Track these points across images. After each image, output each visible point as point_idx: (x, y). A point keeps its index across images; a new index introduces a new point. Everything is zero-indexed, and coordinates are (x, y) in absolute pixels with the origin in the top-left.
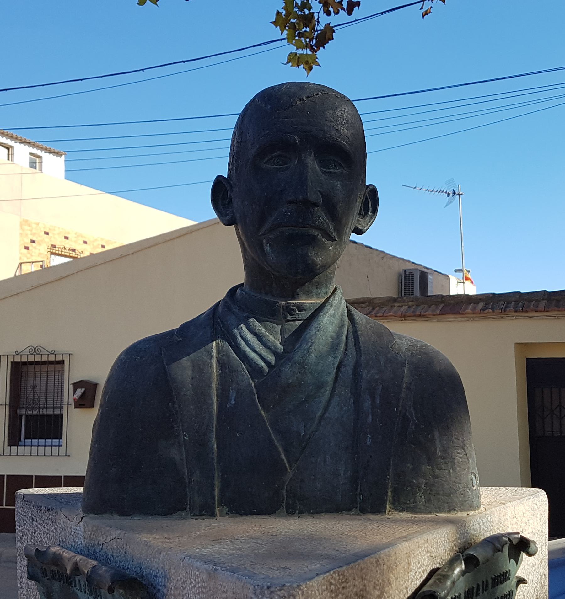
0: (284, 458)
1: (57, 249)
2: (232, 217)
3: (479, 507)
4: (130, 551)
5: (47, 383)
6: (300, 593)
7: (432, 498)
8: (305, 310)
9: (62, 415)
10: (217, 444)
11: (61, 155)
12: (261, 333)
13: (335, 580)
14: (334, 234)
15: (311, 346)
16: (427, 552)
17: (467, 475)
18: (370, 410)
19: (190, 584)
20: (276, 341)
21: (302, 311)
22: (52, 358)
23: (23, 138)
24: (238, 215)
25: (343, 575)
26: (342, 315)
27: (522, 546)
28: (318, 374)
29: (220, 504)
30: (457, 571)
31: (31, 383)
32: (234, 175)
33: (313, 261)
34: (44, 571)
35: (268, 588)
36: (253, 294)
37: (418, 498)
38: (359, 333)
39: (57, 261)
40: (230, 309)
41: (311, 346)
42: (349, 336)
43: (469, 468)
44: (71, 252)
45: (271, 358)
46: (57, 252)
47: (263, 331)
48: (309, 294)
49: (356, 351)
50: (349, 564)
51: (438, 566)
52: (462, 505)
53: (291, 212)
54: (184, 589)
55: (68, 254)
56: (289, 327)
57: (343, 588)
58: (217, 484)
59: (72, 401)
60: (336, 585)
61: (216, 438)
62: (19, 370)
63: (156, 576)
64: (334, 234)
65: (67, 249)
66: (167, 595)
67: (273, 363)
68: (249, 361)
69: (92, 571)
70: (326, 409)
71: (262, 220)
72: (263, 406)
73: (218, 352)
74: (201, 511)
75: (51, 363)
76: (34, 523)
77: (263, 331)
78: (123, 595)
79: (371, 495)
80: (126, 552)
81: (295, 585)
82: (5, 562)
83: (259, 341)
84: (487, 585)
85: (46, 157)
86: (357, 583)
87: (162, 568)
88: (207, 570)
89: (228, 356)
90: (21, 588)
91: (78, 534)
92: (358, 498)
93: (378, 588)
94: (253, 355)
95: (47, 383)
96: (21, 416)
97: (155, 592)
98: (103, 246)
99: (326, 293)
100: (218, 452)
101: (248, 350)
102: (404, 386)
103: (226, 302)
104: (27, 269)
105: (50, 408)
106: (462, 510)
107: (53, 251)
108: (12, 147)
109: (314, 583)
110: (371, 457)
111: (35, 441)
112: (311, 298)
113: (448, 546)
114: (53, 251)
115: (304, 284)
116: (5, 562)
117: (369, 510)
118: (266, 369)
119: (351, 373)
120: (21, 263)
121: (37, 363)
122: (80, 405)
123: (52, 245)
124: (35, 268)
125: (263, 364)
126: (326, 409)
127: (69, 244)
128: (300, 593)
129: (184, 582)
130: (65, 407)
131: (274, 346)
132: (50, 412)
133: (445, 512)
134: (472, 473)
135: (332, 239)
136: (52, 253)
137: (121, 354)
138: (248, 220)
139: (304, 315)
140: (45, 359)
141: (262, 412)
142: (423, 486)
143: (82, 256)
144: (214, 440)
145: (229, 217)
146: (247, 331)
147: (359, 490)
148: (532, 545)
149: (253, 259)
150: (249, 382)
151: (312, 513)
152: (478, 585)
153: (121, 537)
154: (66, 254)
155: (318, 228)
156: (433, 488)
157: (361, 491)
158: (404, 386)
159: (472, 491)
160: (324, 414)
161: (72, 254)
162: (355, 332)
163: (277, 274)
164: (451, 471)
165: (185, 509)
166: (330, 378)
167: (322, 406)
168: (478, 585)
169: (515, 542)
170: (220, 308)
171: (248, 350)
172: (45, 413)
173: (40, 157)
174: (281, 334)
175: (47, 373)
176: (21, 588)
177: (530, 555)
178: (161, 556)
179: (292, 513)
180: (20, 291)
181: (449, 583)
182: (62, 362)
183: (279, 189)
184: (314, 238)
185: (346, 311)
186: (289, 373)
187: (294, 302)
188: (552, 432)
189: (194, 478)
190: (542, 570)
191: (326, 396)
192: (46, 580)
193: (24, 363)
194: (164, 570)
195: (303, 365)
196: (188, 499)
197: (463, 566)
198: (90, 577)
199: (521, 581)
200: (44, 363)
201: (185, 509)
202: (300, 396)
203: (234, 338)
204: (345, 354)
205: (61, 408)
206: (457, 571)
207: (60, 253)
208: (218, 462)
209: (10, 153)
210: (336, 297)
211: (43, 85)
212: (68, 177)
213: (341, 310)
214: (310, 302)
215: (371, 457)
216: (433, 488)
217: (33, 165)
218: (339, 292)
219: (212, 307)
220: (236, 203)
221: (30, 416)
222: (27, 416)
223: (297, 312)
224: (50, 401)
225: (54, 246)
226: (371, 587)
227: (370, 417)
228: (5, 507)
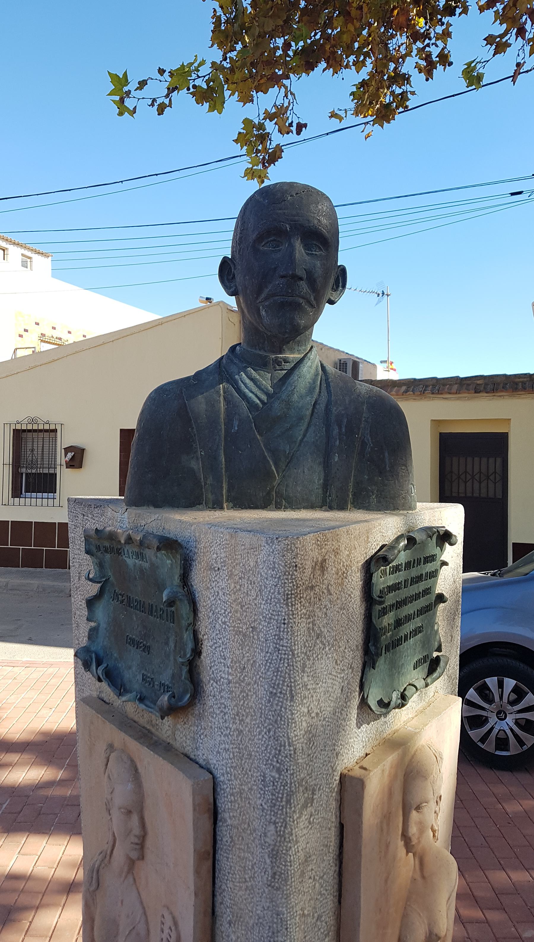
0: (274, 469)
1: (46, 337)
2: (235, 289)
3: (415, 509)
4: (167, 527)
5: (43, 446)
6: (298, 542)
7: (382, 500)
8: (289, 362)
9: (56, 474)
10: (225, 459)
11: (48, 256)
12: (256, 379)
13: (320, 538)
14: (314, 303)
15: (294, 388)
16: (380, 532)
17: (408, 485)
18: (337, 437)
19: (216, 543)
20: (267, 384)
21: (287, 363)
22: (47, 427)
23: (16, 241)
24: (240, 288)
25: (326, 536)
26: (317, 367)
27: (446, 537)
28: (299, 409)
29: (227, 501)
30: (402, 544)
31: (29, 446)
32: (237, 256)
33: (298, 323)
34: (98, 548)
35: (277, 538)
36: (249, 349)
37: (371, 500)
38: (330, 380)
39: (47, 347)
40: (232, 361)
41: (294, 388)
42: (322, 382)
43: (409, 480)
44: (58, 340)
45: (264, 397)
46: (46, 340)
47: (258, 377)
48: (292, 351)
49: (328, 393)
50: (329, 530)
51: (387, 543)
52: (403, 506)
53: (282, 284)
54: (211, 547)
55: (56, 342)
56: (277, 375)
57: (325, 544)
58: (225, 486)
59: (64, 463)
60: (321, 542)
61: (224, 454)
62: (19, 436)
63: (189, 542)
64: (314, 303)
65: (55, 337)
66: (198, 553)
67: (266, 401)
68: (247, 399)
69: (143, 538)
70: (304, 436)
71: (259, 291)
72: (258, 432)
73: (224, 392)
74: (214, 504)
75: (46, 431)
76: (85, 517)
77: (258, 377)
78: (165, 555)
79: (337, 497)
80: (164, 529)
81: (295, 537)
82: (11, 590)
83: (255, 385)
84: (420, 562)
85: (35, 257)
86: (334, 543)
87: (194, 535)
88: (229, 533)
89: (232, 395)
90: (74, 566)
91: (123, 521)
92: (327, 498)
93: (347, 549)
94: (251, 395)
95: (43, 446)
96: (22, 474)
97: (188, 552)
98: (84, 336)
99: (305, 350)
100: (225, 465)
101: (247, 391)
102: (364, 419)
103: (229, 356)
104: (20, 353)
105: (46, 468)
106: (403, 510)
107: (43, 339)
108: (7, 249)
109: (307, 537)
110: (338, 470)
111: (34, 495)
112: (293, 353)
113: (394, 531)
114: (43, 339)
115: (288, 343)
116: (11, 590)
117: (335, 507)
118: (261, 406)
119: (323, 410)
120: (16, 349)
121: (35, 431)
122: (70, 466)
123: (42, 334)
124: (29, 352)
125: (258, 402)
126: (304, 436)
127: (56, 334)
128: (298, 542)
129: (211, 543)
130: (58, 467)
131: (266, 389)
132: (46, 471)
133: (391, 510)
134: (412, 484)
135: (312, 306)
136: (42, 341)
137: (151, 393)
138: (248, 291)
139: (288, 366)
140: (41, 427)
141: (258, 436)
142: (375, 492)
143: (67, 343)
144: (223, 456)
145: (232, 289)
146: (246, 377)
147: (328, 493)
148: (453, 537)
149: (250, 322)
150: (248, 414)
151: (294, 509)
152: (414, 560)
153: (159, 518)
154: (53, 342)
155: (303, 298)
156: (383, 493)
157: (330, 493)
158: (364, 419)
159: (411, 497)
160: (303, 439)
161: (59, 342)
162: (327, 380)
163: (269, 334)
164: (396, 482)
165: (202, 504)
166: (309, 413)
167: (302, 433)
168: (414, 560)
169: (441, 533)
170: (224, 361)
171: (247, 391)
172: (41, 471)
173: (30, 258)
174: (271, 380)
175: (43, 440)
176: (74, 566)
177: (451, 544)
178: (193, 528)
179: (279, 508)
180: (19, 371)
181: (396, 551)
182: (55, 431)
183: (273, 267)
184: (299, 305)
185: (320, 364)
186: (277, 407)
187: (281, 356)
188: (458, 493)
189: (208, 482)
190: (458, 562)
191: (305, 426)
192: (99, 553)
193: (24, 431)
194: (195, 537)
195: (288, 403)
196: (204, 496)
197: (406, 542)
198: (142, 541)
199: (444, 563)
200: (41, 431)
201: (202, 504)
202: (286, 425)
203: (236, 382)
204: (319, 395)
205: (55, 468)
206: (402, 544)
207: (49, 341)
208: (226, 471)
209: (6, 253)
210: (313, 353)
211: (38, 195)
212: (53, 276)
213: (316, 363)
214: (293, 356)
215: (338, 470)
216: (383, 493)
217: (24, 265)
218: (314, 349)
219: (217, 360)
220: (239, 278)
221: (30, 474)
222: (27, 474)
223: (283, 364)
224: (46, 462)
225: (43, 335)
226: (343, 548)
227: (338, 441)
228: (9, 546)
